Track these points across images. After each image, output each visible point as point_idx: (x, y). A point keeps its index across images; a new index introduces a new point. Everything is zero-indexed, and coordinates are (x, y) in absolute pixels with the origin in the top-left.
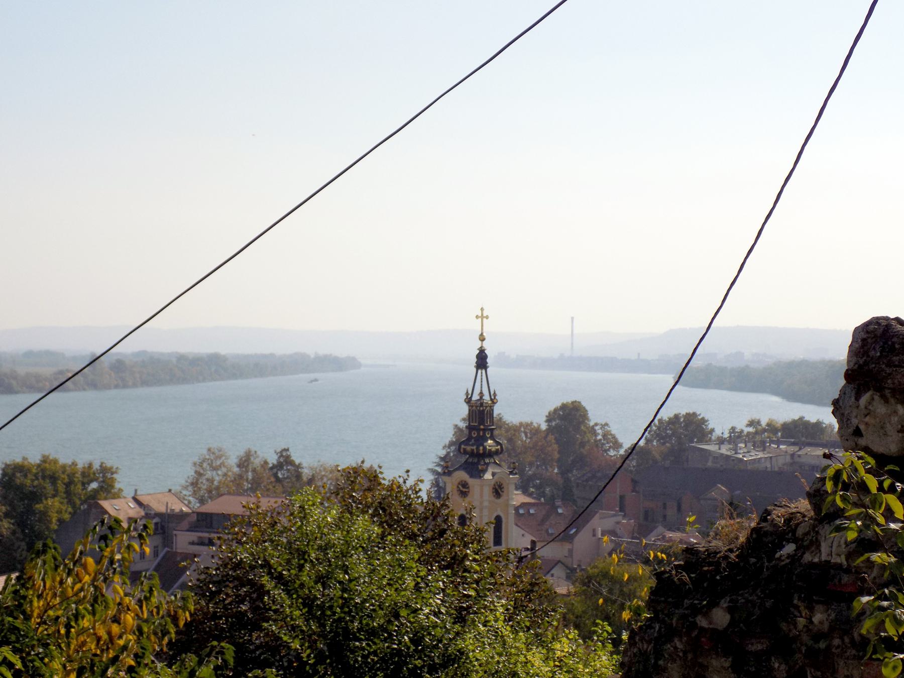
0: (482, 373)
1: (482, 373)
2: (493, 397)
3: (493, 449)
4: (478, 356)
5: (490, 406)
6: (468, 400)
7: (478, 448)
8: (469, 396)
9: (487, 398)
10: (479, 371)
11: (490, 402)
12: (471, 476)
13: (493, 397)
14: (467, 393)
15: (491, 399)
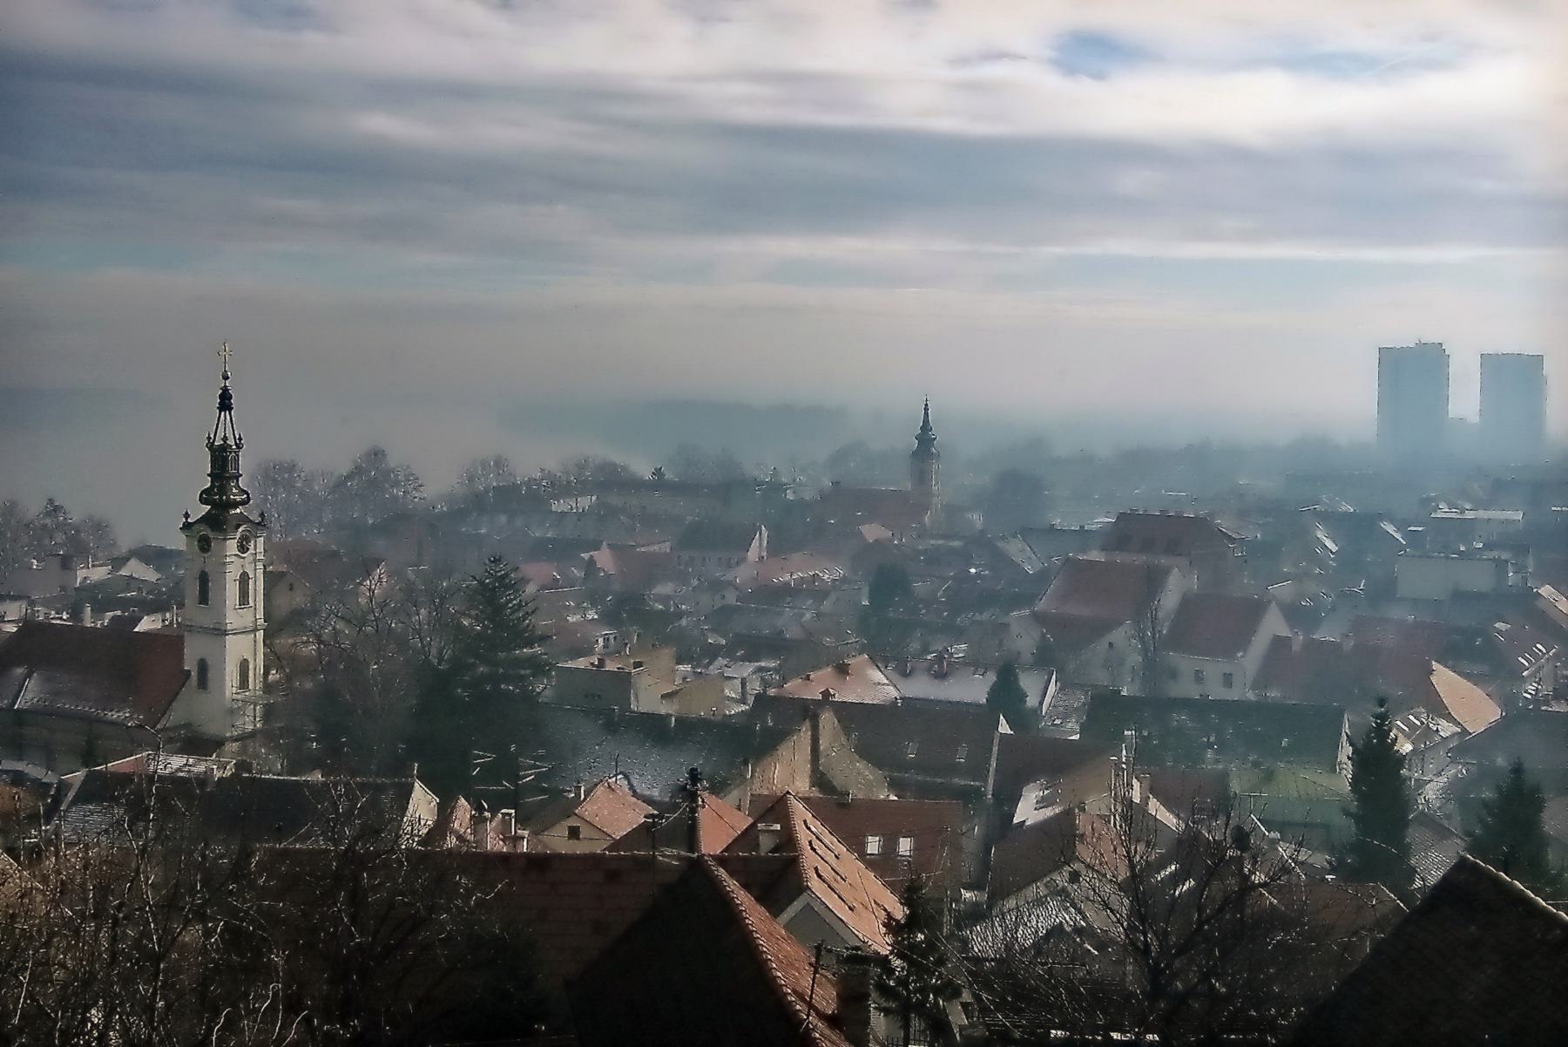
0: (225, 414)
1: (225, 414)
2: (238, 441)
3: (238, 498)
4: (221, 396)
5: (235, 452)
6: (211, 446)
7: (221, 498)
8: (211, 441)
9: (231, 442)
10: (223, 413)
11: (234, 447)
12: (213, 530)
13: (238, 441)
14: (209, 438)
15: (236, 444)
